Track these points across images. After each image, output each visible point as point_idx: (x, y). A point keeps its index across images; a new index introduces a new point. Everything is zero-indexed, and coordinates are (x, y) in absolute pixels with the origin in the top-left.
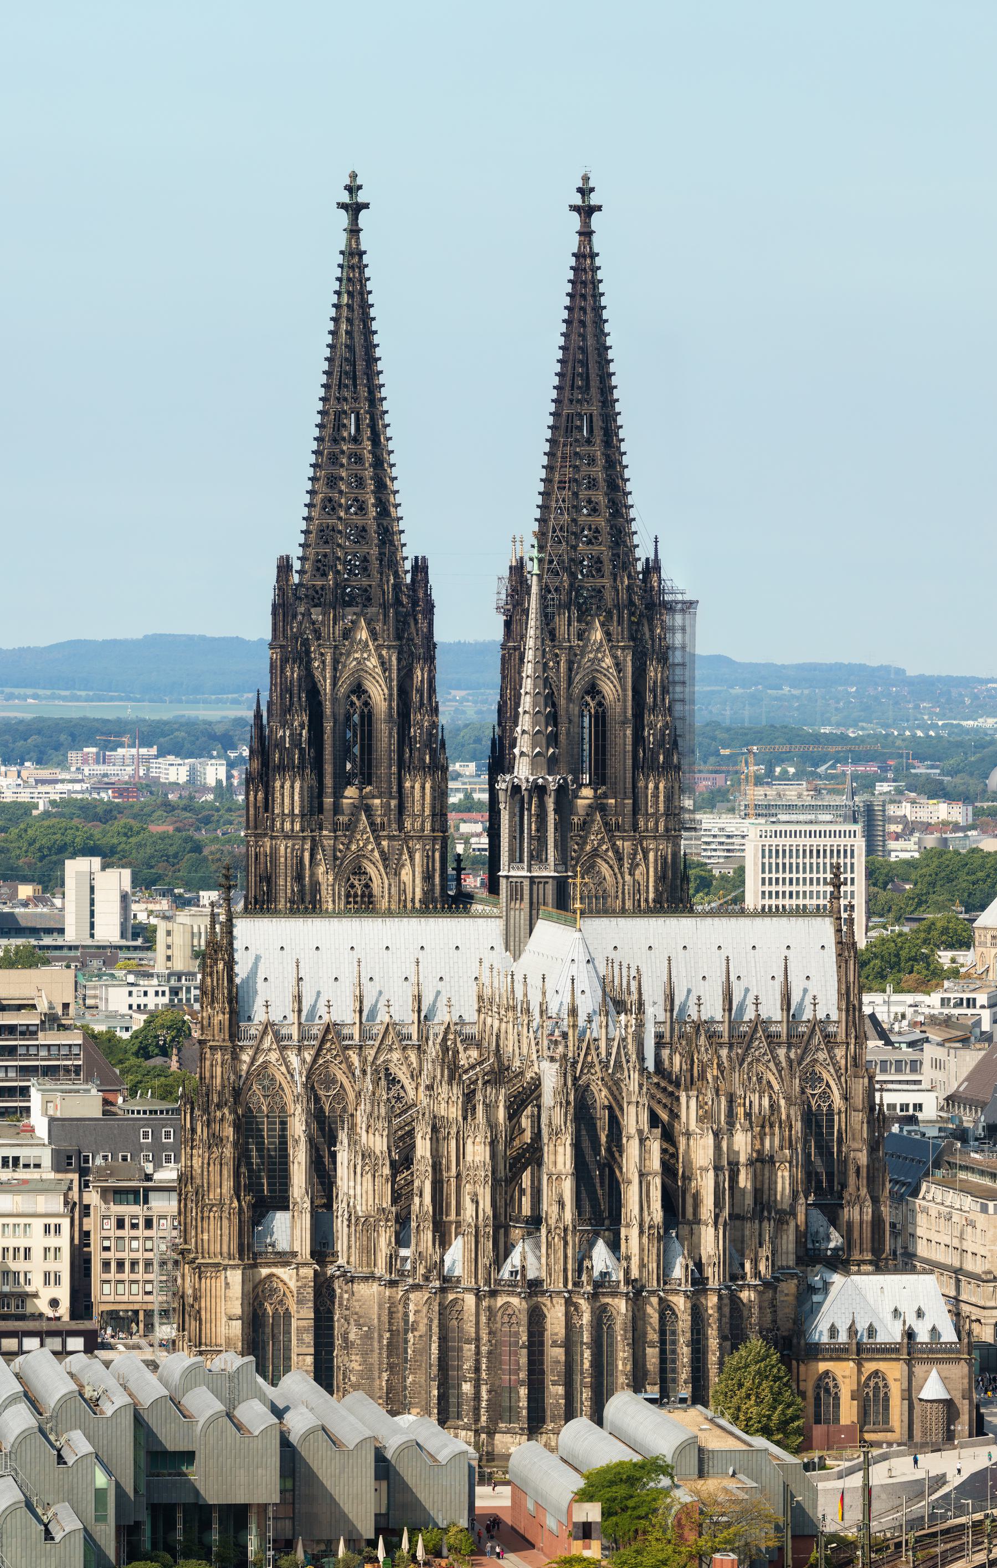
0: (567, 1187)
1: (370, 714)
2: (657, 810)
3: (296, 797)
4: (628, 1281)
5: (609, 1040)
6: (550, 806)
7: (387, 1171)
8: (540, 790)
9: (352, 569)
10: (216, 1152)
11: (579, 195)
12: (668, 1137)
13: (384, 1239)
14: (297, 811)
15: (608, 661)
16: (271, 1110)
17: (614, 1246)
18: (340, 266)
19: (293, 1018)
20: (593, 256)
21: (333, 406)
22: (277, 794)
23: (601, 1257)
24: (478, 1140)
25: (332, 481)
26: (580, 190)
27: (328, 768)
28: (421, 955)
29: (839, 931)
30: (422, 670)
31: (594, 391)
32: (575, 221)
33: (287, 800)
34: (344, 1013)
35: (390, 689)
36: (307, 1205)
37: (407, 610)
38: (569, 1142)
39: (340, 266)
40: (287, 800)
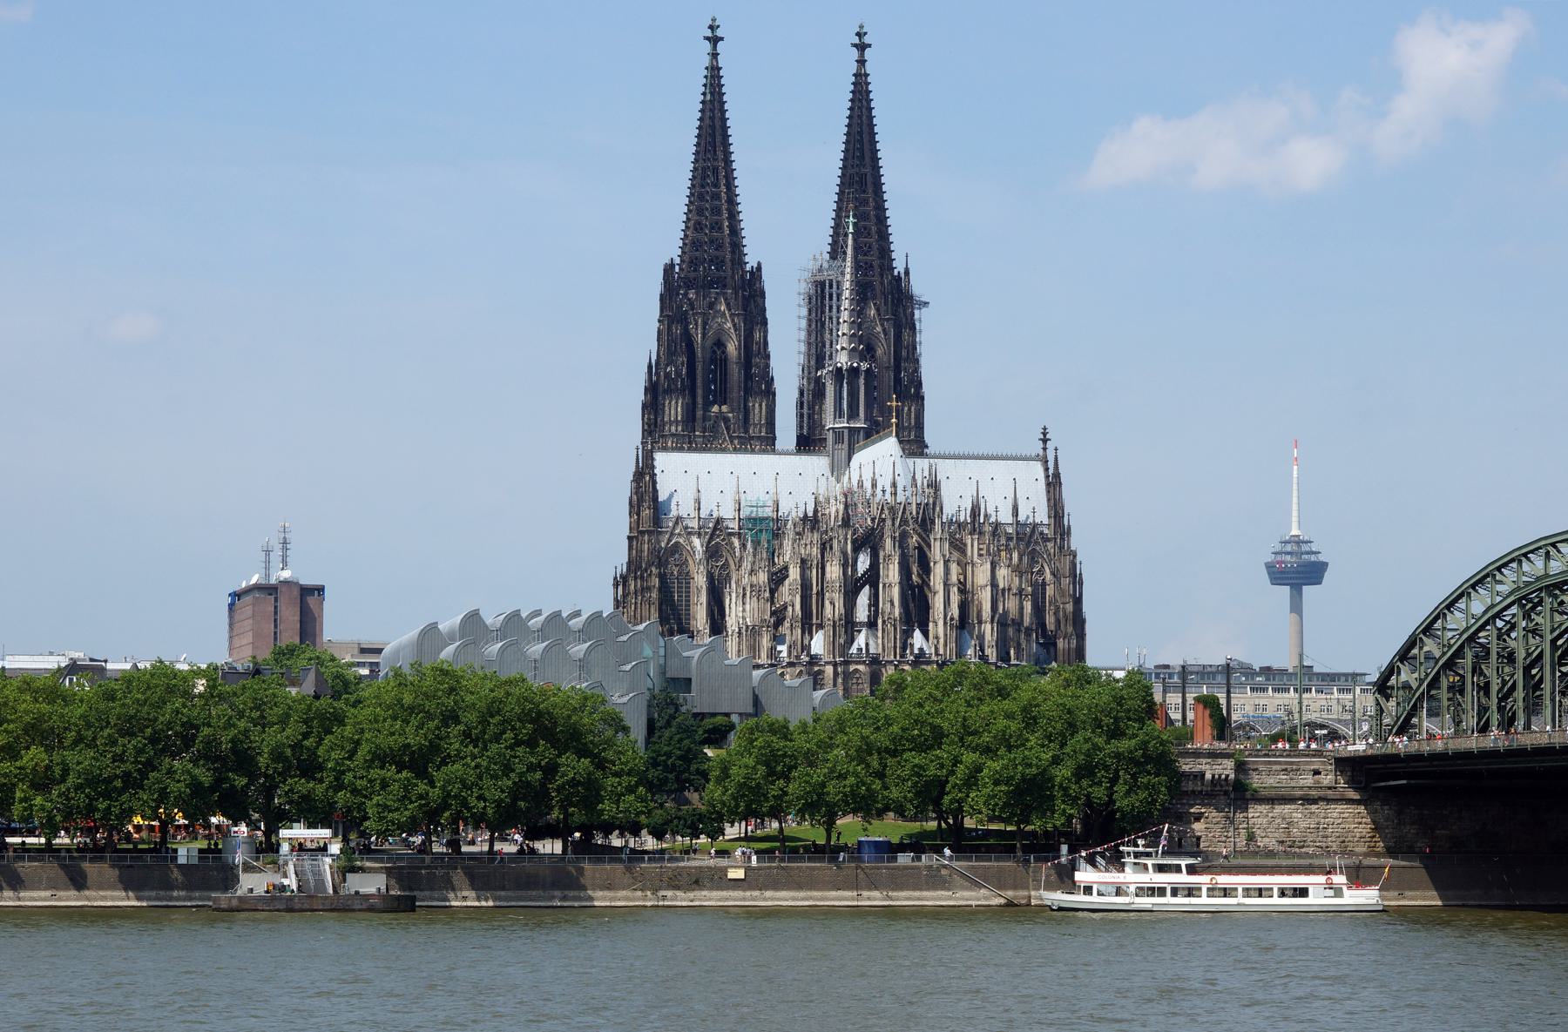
0: (896, 592)
1: (726, 359)
4: (937, 654)
5: (918, 505)
6: (862, 381)
8: (854, 372)
9: (710, 271)
12: (963, 565)
13: (765, 642)
15: (879, 329)
16: (680, 573)
17: (926, 634)
19: (694, 514)
20: (867, 75)
21: (701, 164)
23: (918, 639)
25: (700, 211)
26: (858, 34)
27: (699, 392)
29: (1047, 469)
31: (867, 160)
32: (855, 53)
34: (728, 512)
37: (750, 295)
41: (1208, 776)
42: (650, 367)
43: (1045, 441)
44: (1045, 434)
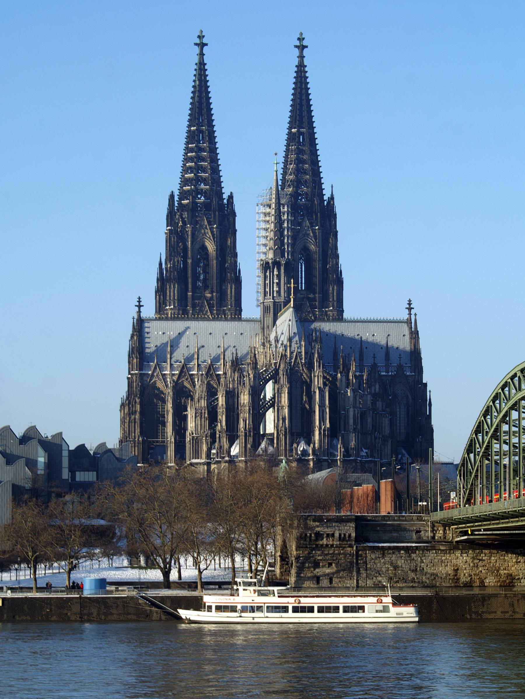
2: (333, 299)
3: (176, 292)
7: (206, 415)
10: (133, 417)
11: (298, 41)
14: (176, 298)
18: (196, 70)
22: (168, 292)
24: (246, 393)
26: (299, 39)
28: (225, 337)
30: (231, 239)
32: (297, 52)
33: (172, 294)
35: (217, 246)
36: (173, 440)
37: (224, 216)
38: (286, 392)
39: (196, 70)
40: (172, 294)
41: (337, 535)
42: (160, 264)
43: (410, 309)
44: (410, 304)
